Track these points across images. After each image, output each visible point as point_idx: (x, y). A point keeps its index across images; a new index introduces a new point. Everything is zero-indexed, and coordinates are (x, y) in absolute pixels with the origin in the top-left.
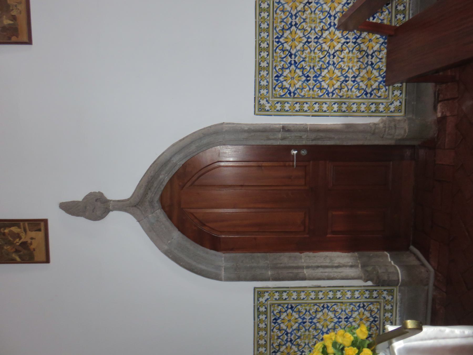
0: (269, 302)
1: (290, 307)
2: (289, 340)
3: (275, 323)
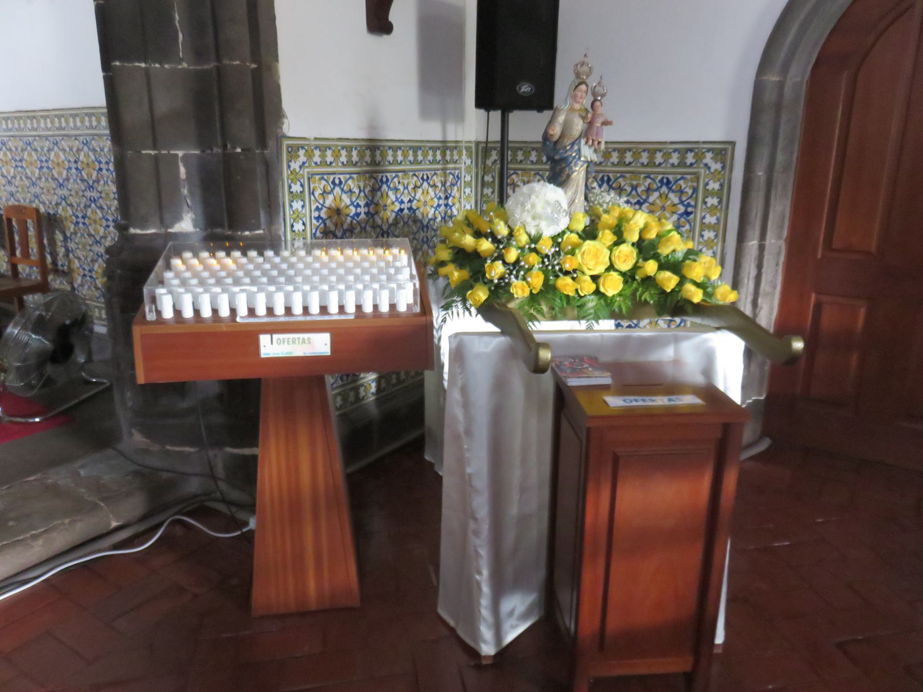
0: (702, 171)
1: (690, 209)
3: (661, 181)
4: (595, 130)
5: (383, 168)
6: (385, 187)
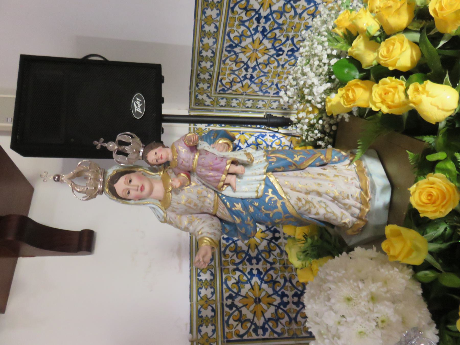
4: (204, 172)
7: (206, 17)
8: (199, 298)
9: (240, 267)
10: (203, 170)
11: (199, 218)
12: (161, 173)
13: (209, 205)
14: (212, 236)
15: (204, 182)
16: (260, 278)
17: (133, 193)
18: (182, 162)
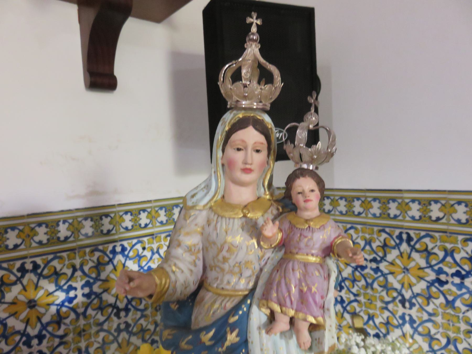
2: (443, 277)
5: (116, 237)
6: (119, 258)
7: (370, 202)
8: (33, 226)
9: (79, 273)
10: (298, 275)
11: (197, 261)
12: (268, 197)
13: (225, 282)
14: (170, 291)
15: (265, 270)
16: (63, 302)
17: (239, 157)
18: (306, 237)
